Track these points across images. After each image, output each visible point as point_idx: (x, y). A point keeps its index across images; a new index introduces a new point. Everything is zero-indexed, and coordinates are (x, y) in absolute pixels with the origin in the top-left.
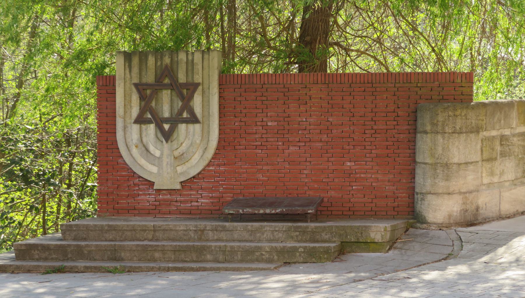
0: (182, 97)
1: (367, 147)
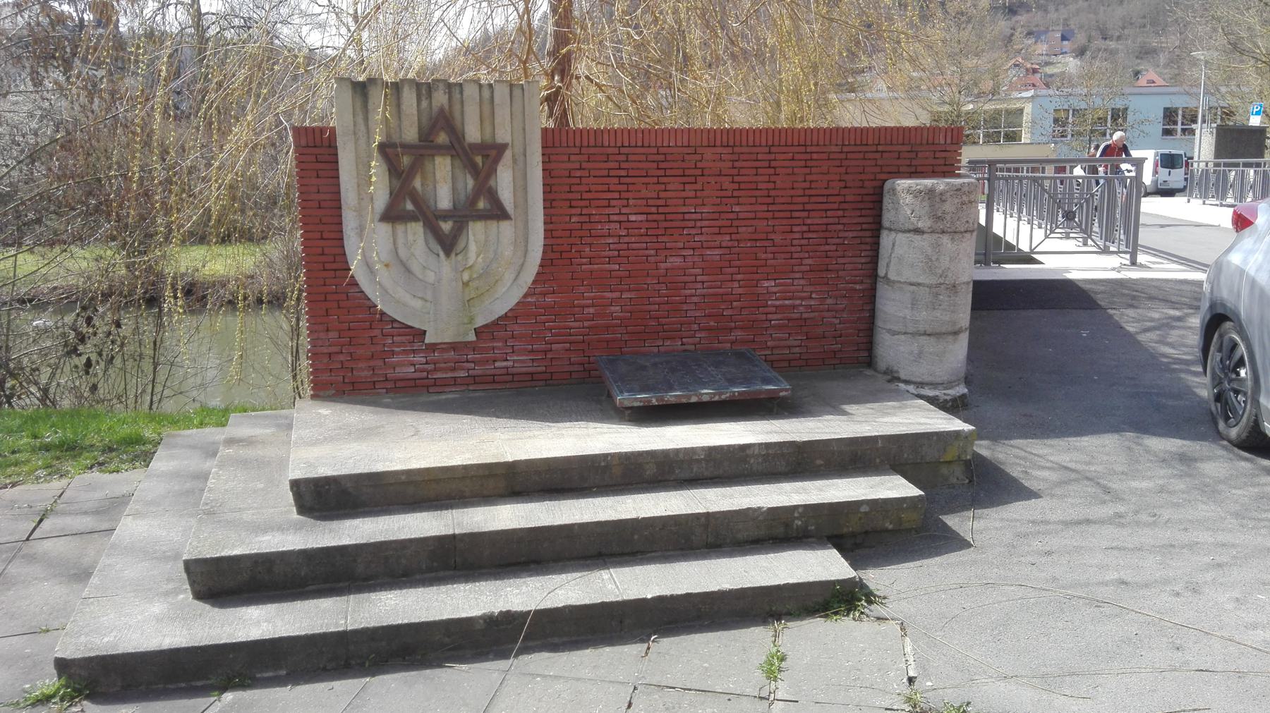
0: (475, 171)
1: (795, 255)
